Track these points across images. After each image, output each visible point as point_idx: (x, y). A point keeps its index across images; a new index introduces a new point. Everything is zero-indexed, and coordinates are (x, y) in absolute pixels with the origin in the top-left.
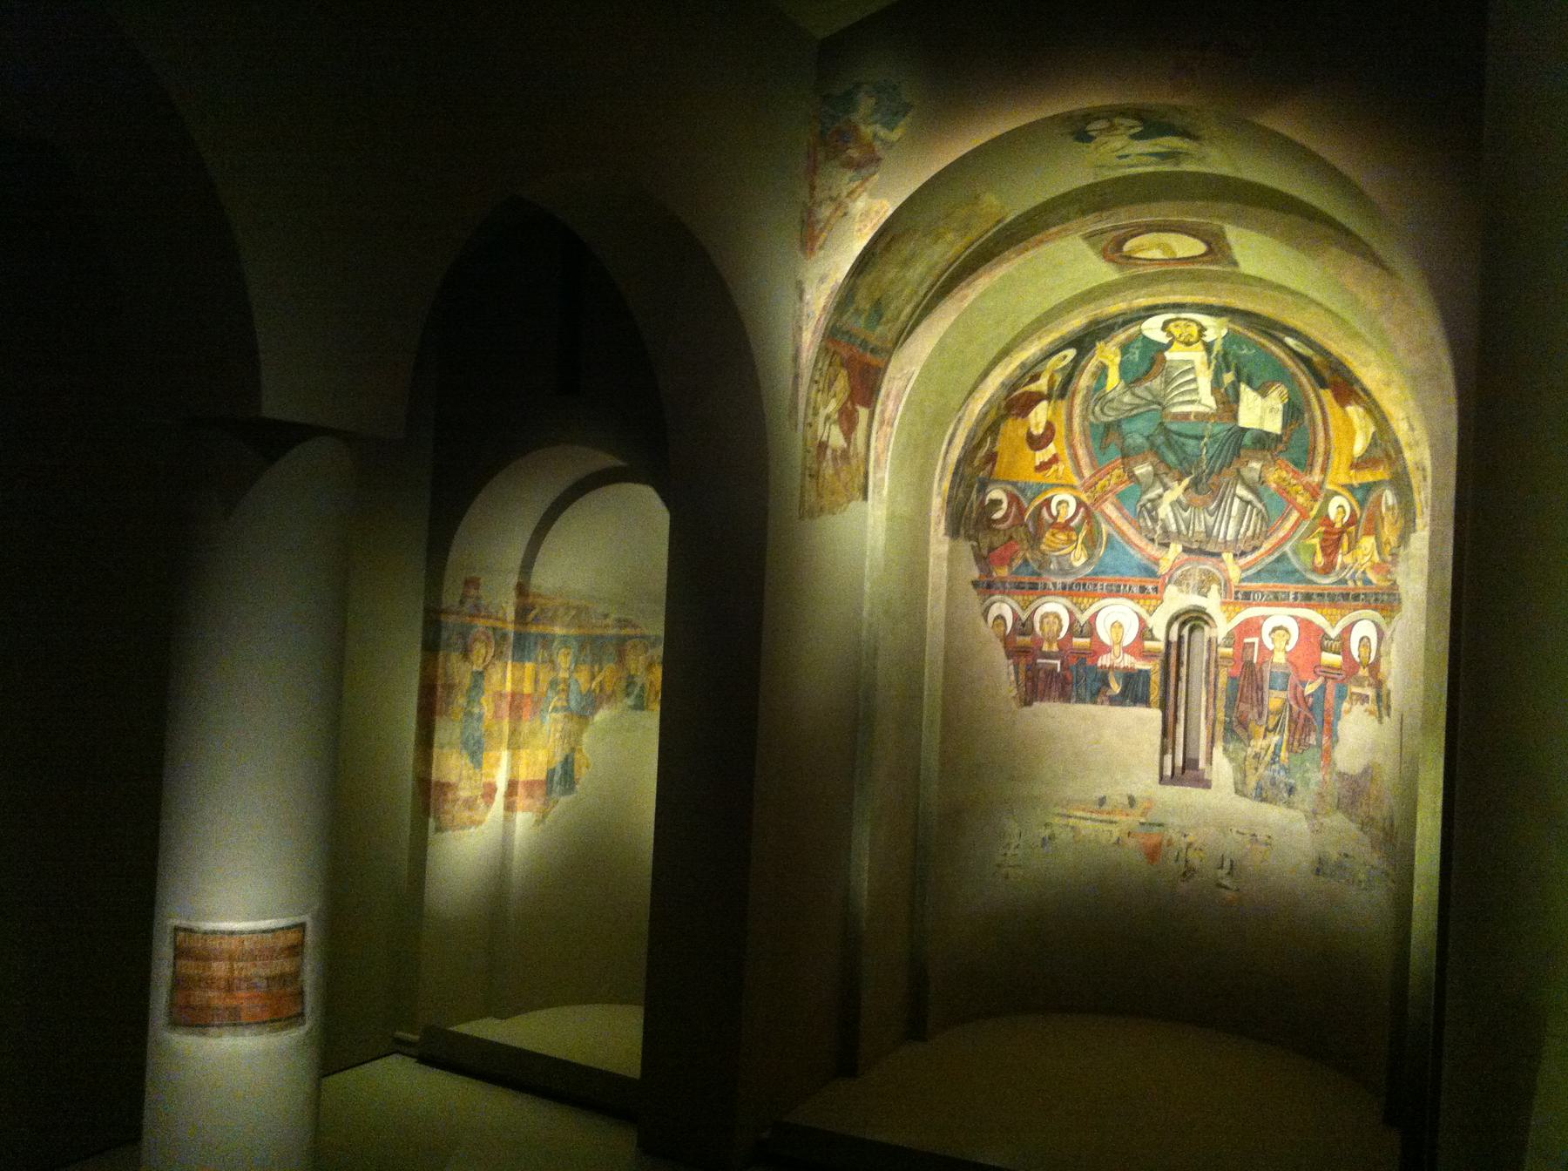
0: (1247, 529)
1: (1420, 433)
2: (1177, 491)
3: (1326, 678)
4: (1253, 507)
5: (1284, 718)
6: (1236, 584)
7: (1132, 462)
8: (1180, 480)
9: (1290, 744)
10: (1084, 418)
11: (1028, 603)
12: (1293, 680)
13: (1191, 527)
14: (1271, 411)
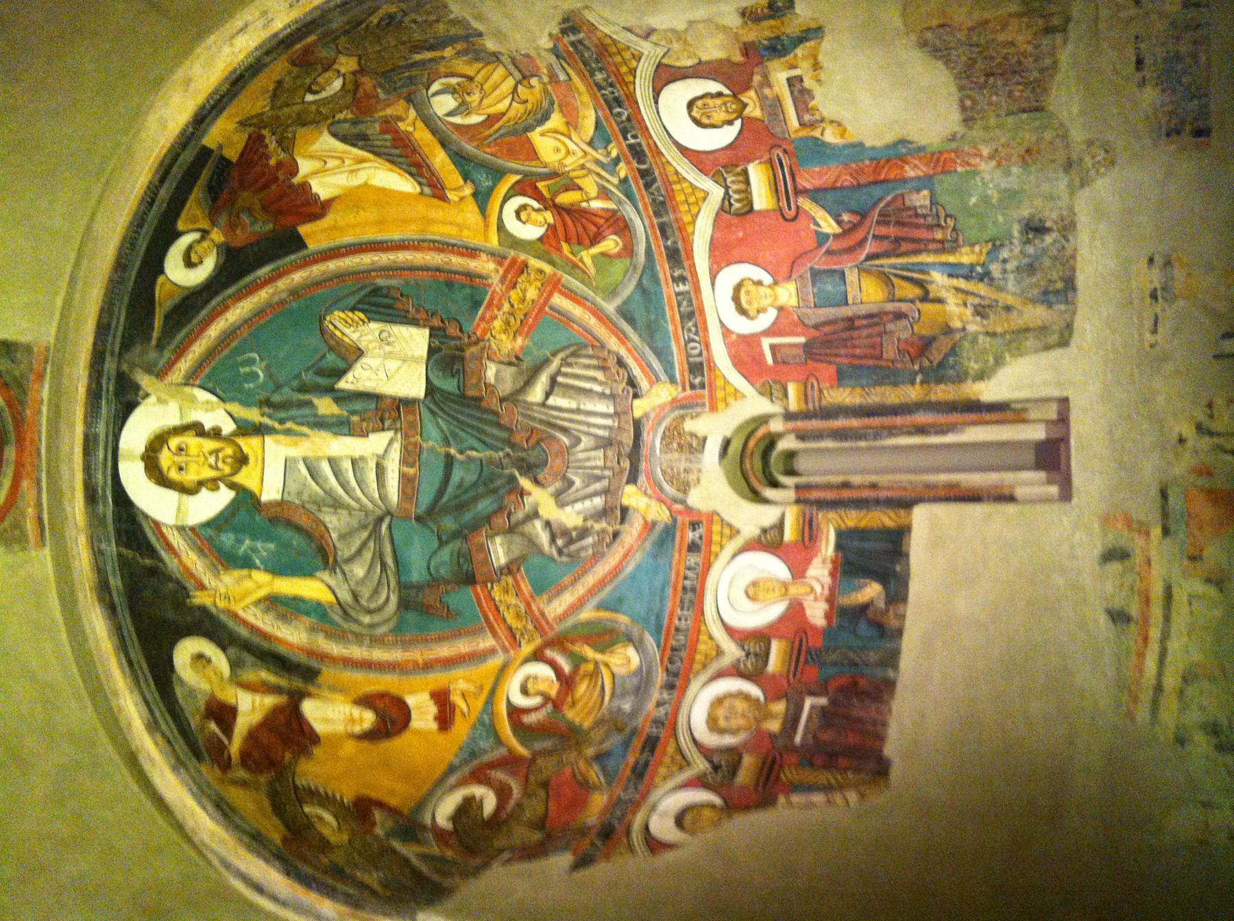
0: (594, 380)
1: (247, 15)
2: (540, 498)
3: (799, 192)
4: (559, 372)
5: (894, 267)
6: (680, 389)
7: (485, 570)
8: (522, 493)
9: (944, 247)
11: (679, 757)
12: (819, 261)
13: (598, 472)
14: (388, 344)
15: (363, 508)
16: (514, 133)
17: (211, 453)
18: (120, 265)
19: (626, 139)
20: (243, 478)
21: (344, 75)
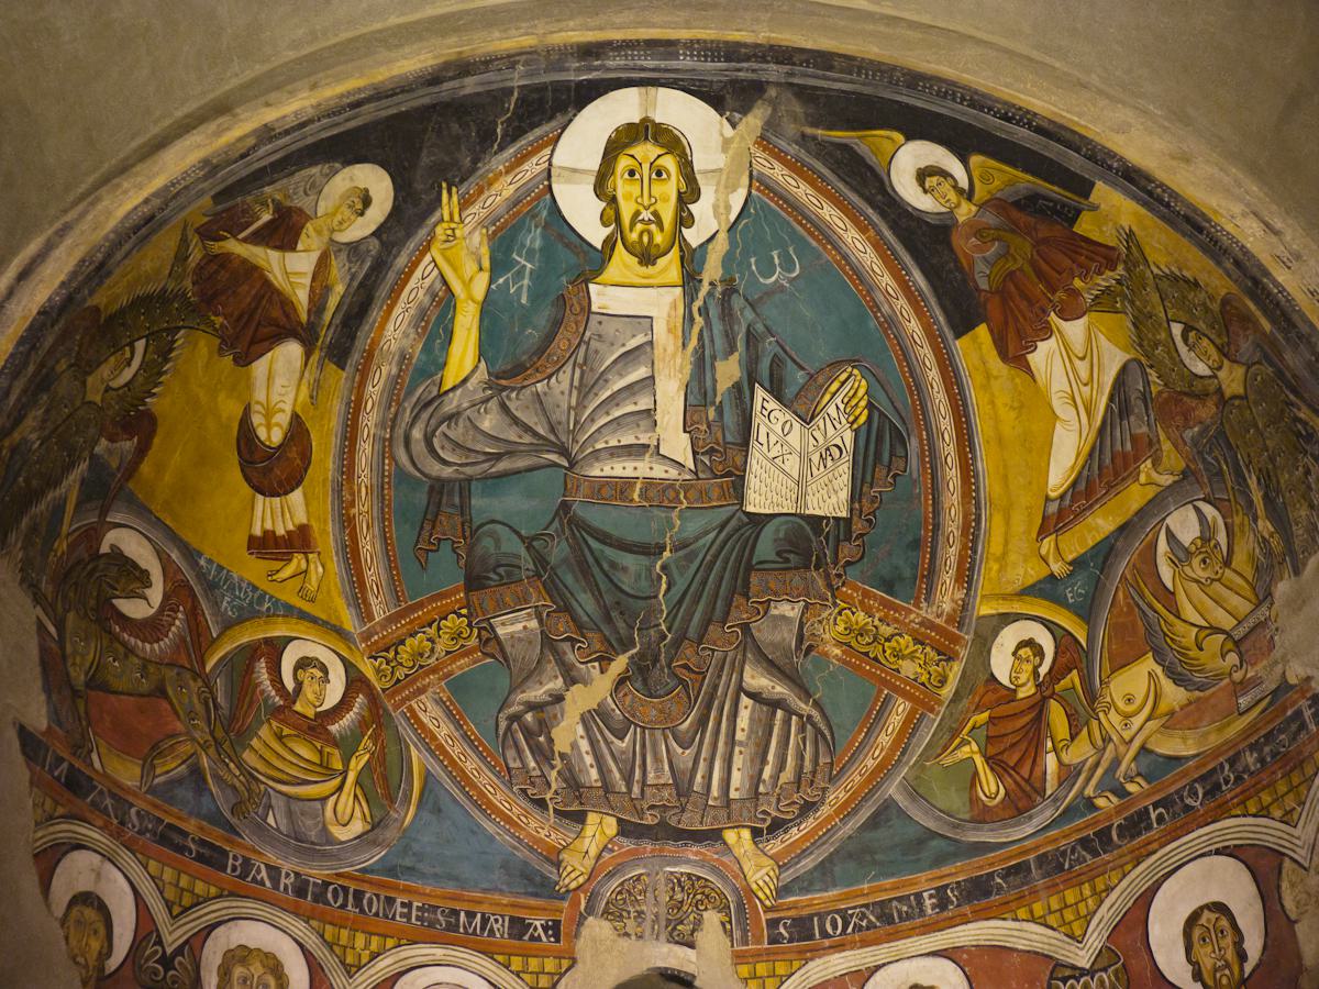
0: (781, 766)
1: (1293, 234)
2: (597, 688)
4: (789, 712)
7: (489, 604)
8: (604, 661)
10: (385, 448)
11: (186, 901)
15: (580, 426)
16: (1150, 631)
17: (655, 214)
18: (915, 80)
19: (1156, 805)
20: (622, 259)
21: (1215, 377)
